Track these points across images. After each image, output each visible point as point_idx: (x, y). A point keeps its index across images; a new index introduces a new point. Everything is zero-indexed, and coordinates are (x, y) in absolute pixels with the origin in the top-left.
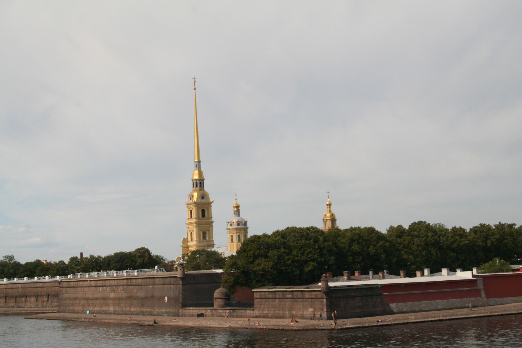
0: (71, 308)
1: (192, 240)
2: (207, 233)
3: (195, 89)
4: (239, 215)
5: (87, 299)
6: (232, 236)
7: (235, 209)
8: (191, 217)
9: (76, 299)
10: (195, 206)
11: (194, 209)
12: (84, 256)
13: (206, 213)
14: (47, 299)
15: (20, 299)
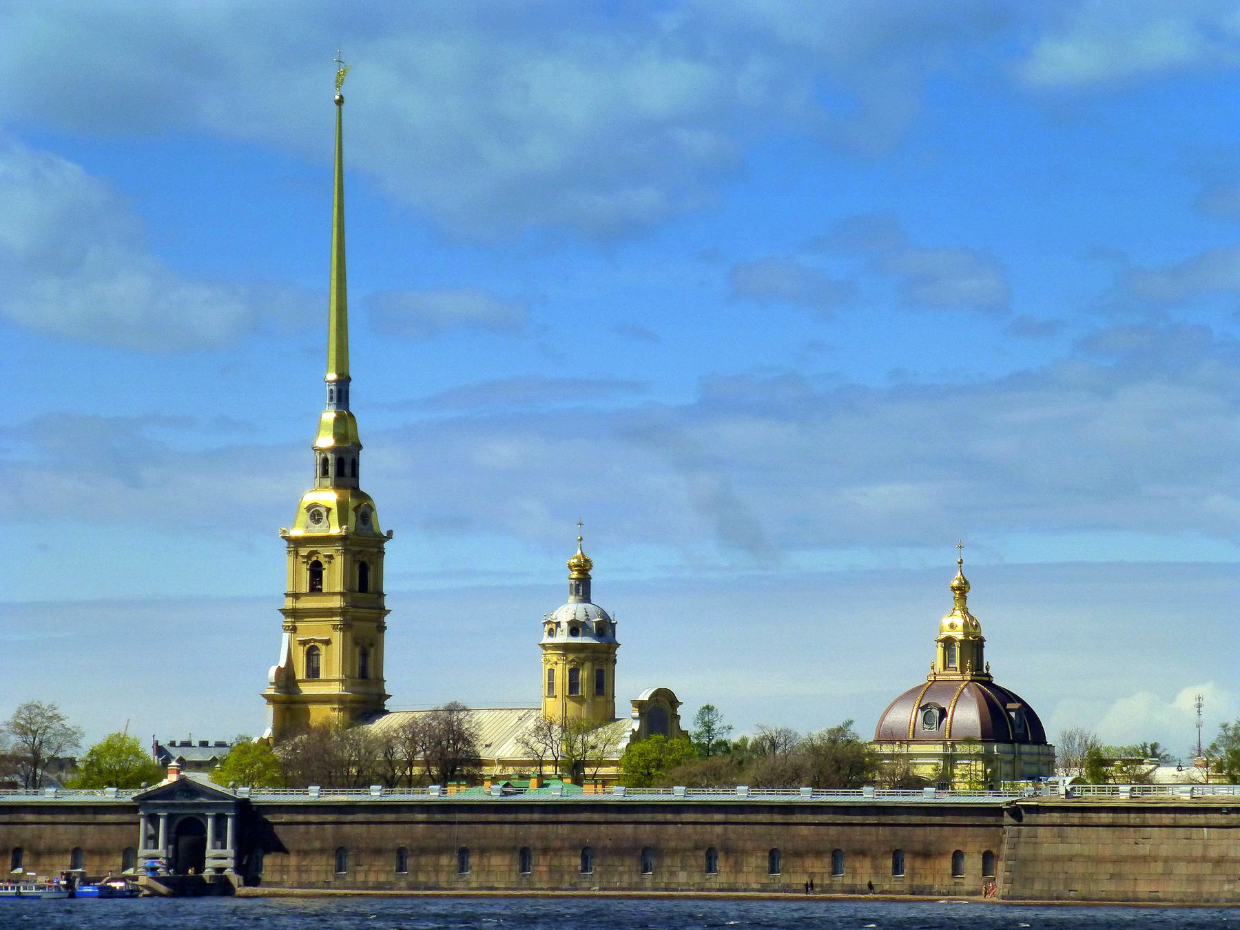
0: (1108, 887)
1: (313, 673)
2: (372, 651)
3: (340, 102)
4: (586, 598)
5: (1219, 861)
6: (551, 671)
7: (575, 575)
8: (316, 586)
9: (1144, 859)
10: (346, 552)
11: (339, 560)
12: (853, 728)
13: (371, 575)
14: (577, 861)
15: (423, 860)
